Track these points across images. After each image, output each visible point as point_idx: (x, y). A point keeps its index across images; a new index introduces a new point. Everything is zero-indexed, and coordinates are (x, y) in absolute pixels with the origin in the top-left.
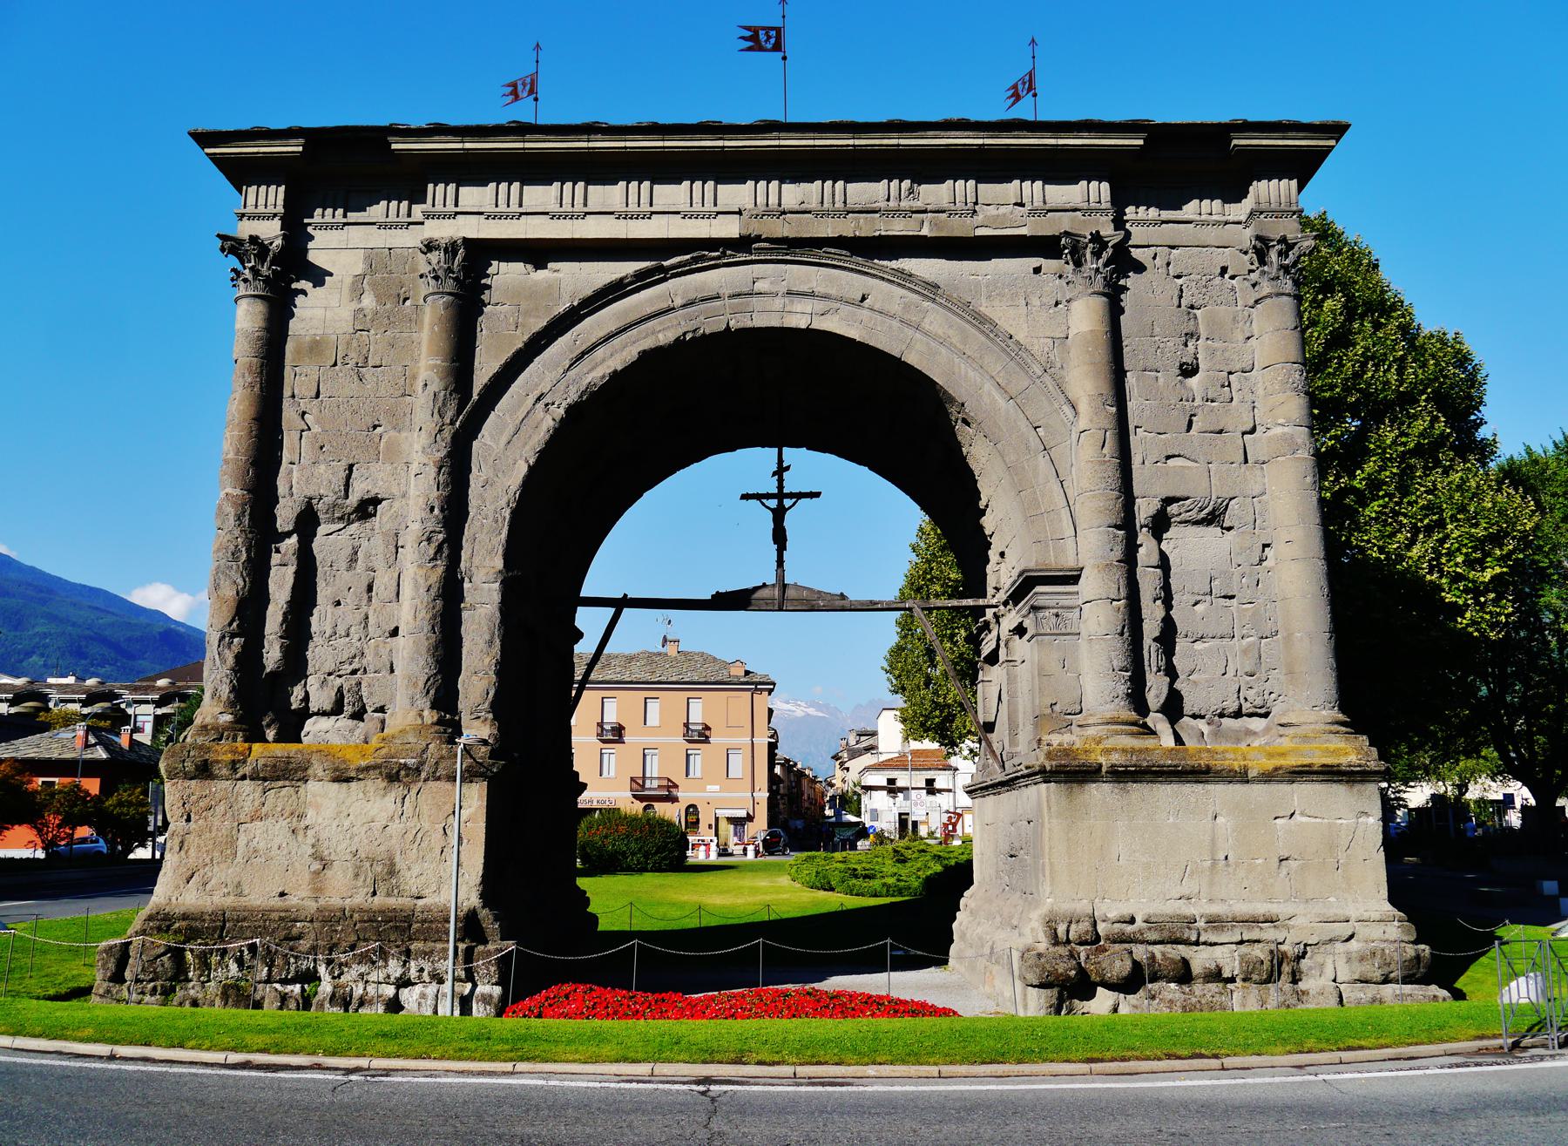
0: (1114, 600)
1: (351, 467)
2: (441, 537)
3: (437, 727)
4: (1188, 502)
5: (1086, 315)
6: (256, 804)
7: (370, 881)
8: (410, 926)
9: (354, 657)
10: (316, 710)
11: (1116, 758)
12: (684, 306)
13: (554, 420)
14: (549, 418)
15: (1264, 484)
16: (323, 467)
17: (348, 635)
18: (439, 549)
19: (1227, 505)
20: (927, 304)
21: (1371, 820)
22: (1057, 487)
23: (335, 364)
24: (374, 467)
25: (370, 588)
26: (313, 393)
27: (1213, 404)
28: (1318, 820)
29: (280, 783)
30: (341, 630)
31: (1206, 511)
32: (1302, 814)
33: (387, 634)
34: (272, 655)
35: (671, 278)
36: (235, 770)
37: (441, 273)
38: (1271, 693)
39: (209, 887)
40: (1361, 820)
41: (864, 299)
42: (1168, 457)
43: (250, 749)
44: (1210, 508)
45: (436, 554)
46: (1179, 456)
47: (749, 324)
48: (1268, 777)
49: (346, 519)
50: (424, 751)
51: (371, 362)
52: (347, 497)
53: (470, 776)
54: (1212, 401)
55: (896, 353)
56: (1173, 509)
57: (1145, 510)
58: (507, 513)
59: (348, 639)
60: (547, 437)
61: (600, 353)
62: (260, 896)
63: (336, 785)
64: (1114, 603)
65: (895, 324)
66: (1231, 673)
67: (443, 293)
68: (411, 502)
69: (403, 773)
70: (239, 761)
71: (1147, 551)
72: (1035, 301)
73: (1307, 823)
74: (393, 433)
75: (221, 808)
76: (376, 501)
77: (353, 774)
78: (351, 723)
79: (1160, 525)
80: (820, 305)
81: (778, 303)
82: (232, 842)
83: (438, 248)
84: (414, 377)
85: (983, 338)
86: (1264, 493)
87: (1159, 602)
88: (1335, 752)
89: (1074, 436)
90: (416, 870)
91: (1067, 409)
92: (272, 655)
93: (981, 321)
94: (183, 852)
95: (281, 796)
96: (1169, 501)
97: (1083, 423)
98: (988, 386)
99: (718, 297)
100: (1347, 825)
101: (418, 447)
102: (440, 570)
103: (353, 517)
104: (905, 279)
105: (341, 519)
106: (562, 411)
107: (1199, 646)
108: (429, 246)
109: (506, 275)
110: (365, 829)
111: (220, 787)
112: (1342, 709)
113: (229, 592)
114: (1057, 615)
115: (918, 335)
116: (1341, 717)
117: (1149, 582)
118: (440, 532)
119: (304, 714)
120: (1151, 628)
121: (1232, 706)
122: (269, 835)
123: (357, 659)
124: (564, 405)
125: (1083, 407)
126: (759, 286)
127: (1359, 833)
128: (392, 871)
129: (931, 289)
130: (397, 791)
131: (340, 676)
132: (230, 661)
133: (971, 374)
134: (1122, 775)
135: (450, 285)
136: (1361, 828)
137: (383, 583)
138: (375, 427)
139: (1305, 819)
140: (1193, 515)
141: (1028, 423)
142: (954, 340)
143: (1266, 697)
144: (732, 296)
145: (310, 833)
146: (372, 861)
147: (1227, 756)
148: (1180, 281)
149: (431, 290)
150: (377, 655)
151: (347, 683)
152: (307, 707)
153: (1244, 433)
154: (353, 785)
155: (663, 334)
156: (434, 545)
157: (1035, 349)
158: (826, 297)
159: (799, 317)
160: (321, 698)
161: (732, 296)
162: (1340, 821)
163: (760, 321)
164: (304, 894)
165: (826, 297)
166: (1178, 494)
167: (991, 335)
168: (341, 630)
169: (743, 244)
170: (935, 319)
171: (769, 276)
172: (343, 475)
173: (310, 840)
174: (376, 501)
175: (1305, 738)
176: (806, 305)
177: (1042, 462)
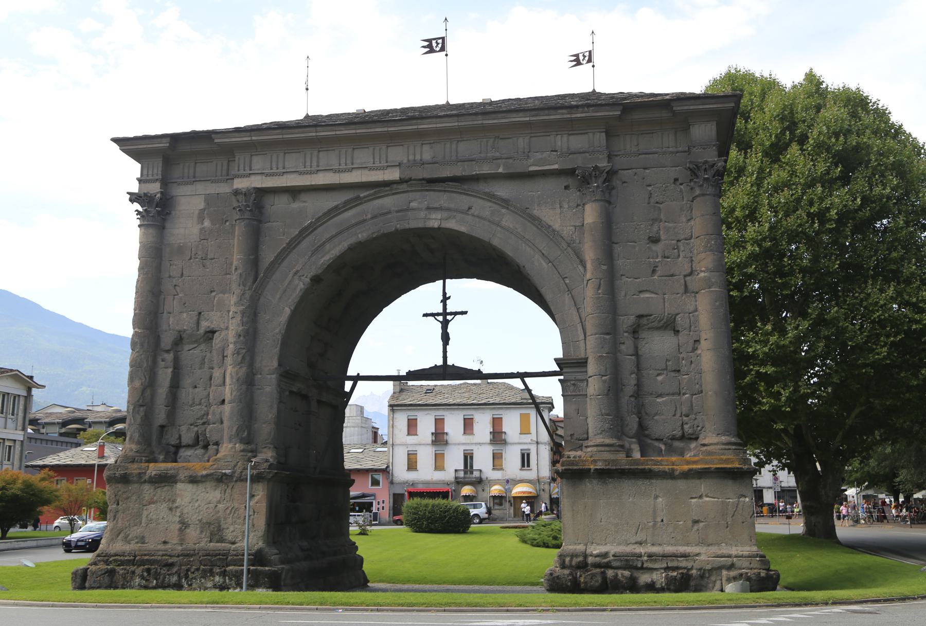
0: (603, 376)
1: (200, 313)
2: (244, 351)
3: (242, 453)
4: (651, 317)
5: (591, 214)
6: (151, 495)
7: (208, 534)
8: (227, 558)
9: (203, 416)
10: (184, 444)
11: (600, 466)
12: (372, 218)
13: (304, 284)
14: (301, 283)
15: (696, 306)
16: (185, 315)
17: (200, 404)
18: (243, 358)
19: (675, 318)
20: (504, 211)
21: (747, 499)
22: (575, 312)
23: (191, 259)
24: (211, 314)
25: (211, 379)
26: (179, 275)
27: (668, 260)
28: (716, 500)
29: (163, 484)
30: (197, 401)
31: (662, 322)
32: (707, 496)
33: (219, 404)
34: (160, 417)
35: (365, 203)
36: (141, 478)
37: (243, 208)
38: (698, 426)
39: (128, 539)
40: (741, 499)
41: (470, 208)
42: (640, 292)
43: (148, 466)
44: (665, 320)
45: (241, 360)
46: (647, 291)
47: (407, 226)
48: (687, 475)
49: (197, 342)
50: (235, 466)
51: (209, 257)
52: (198, 330)
53: (256, 479)
54: (668, 258)
55: (486, 239)
56: (644, 321)
57: (626, 321)
58: (280, 337)
59: (200, 407)
60: (300, 294)
61: (328, 246)
62: (153, 545)
63: (191, 485)
64: (604, 378)
65: (487, 223)
66: (678, 414)
67: (245, 219)
68: (230, 332)
69: (224, 477)
70: (143, 473)
71: (627, 347)
72: (566, 206)
73: (709, 501)
74: (221, 295)
75: (134, 498)
76: (213, 332)
77: (199, 479)
78: (202, 451)
79: (635, 331)
80: (445, 214)
81: (422, 214)
82: (139, 515)
83: (241, 193)
84: (231, 264)
85: (535, 229)
86: (696, 310)
87: (633, 376)
88: (727, 461)
89: (585, 282)
90: (231, 529)
91: (580, 267)
92: (160, 417)
93: (535, 220)
94: (115, 522)
95: (163, 492)
96: (640, 317)
97: (588, 276)
98: (537, 256)
99: (389, 212)
100: (733, 502)
101: (232, 303)
102: (244, 369)
103: (202, 340)
104: (491, 197)
105: (196, 341)
106: (308, 280)
107: (659, 400)
108: (236, 193)
109: (278, 206)
110: (205, 507)
111: (134, 487)
112: (739, 436)
113: (137, 384)
114: (574, 385)
115: (499, 228)
116: (739, 441)
117: (628, 362)
118: (244, 349)
119: (178, 447)
120: (630, 389)
121: (678, 433)
122: (158, 512)
123: (205, 417)
124: (309, 276)
125: (589, 266)
126: (414, 205)
127: (740, 506)
128: (220, 529)
129: (505, 203)
130: (222, 486)
131: (197, 426)
132: (139, 420)
133: (528, 249)
134: (605, 475)
135: (247, 215)
136: (741, 504)
137: (217, 374)
138: (211, 292)
139: (708, 499)
140: (655, 324)
141: (559, 276)
142: (519, 230)
143: (695, 429)
144: (398, 211)
145: (178, 510)
146: (209, 524)
147: (663, 463)
148: (650, 188)
149: (238, 217)
150: (214, 414)
151: (200, 429)
152: (180, 442)
153: (685, 276)
154: (200, 485)
155: (362, 235)
156: (240, 356)
157: (565, 234)
158: (448, 209)
159: (435, 221)
160: (187, 438)
161: (398, 211)
162: (729, 500)
163: (413, 224)
164: (175, 542)
165: (448, 209)
166: (645, 313)
167: (539, 227)
168: (197, 401)
169: (401, 181)
170: (508, 220)
171: (417, 201)
172: (195, 318)
173: (178, 514)
174: (213, 332)
175: (710, 453)
176: (438, 215)
177: (567, 298)
